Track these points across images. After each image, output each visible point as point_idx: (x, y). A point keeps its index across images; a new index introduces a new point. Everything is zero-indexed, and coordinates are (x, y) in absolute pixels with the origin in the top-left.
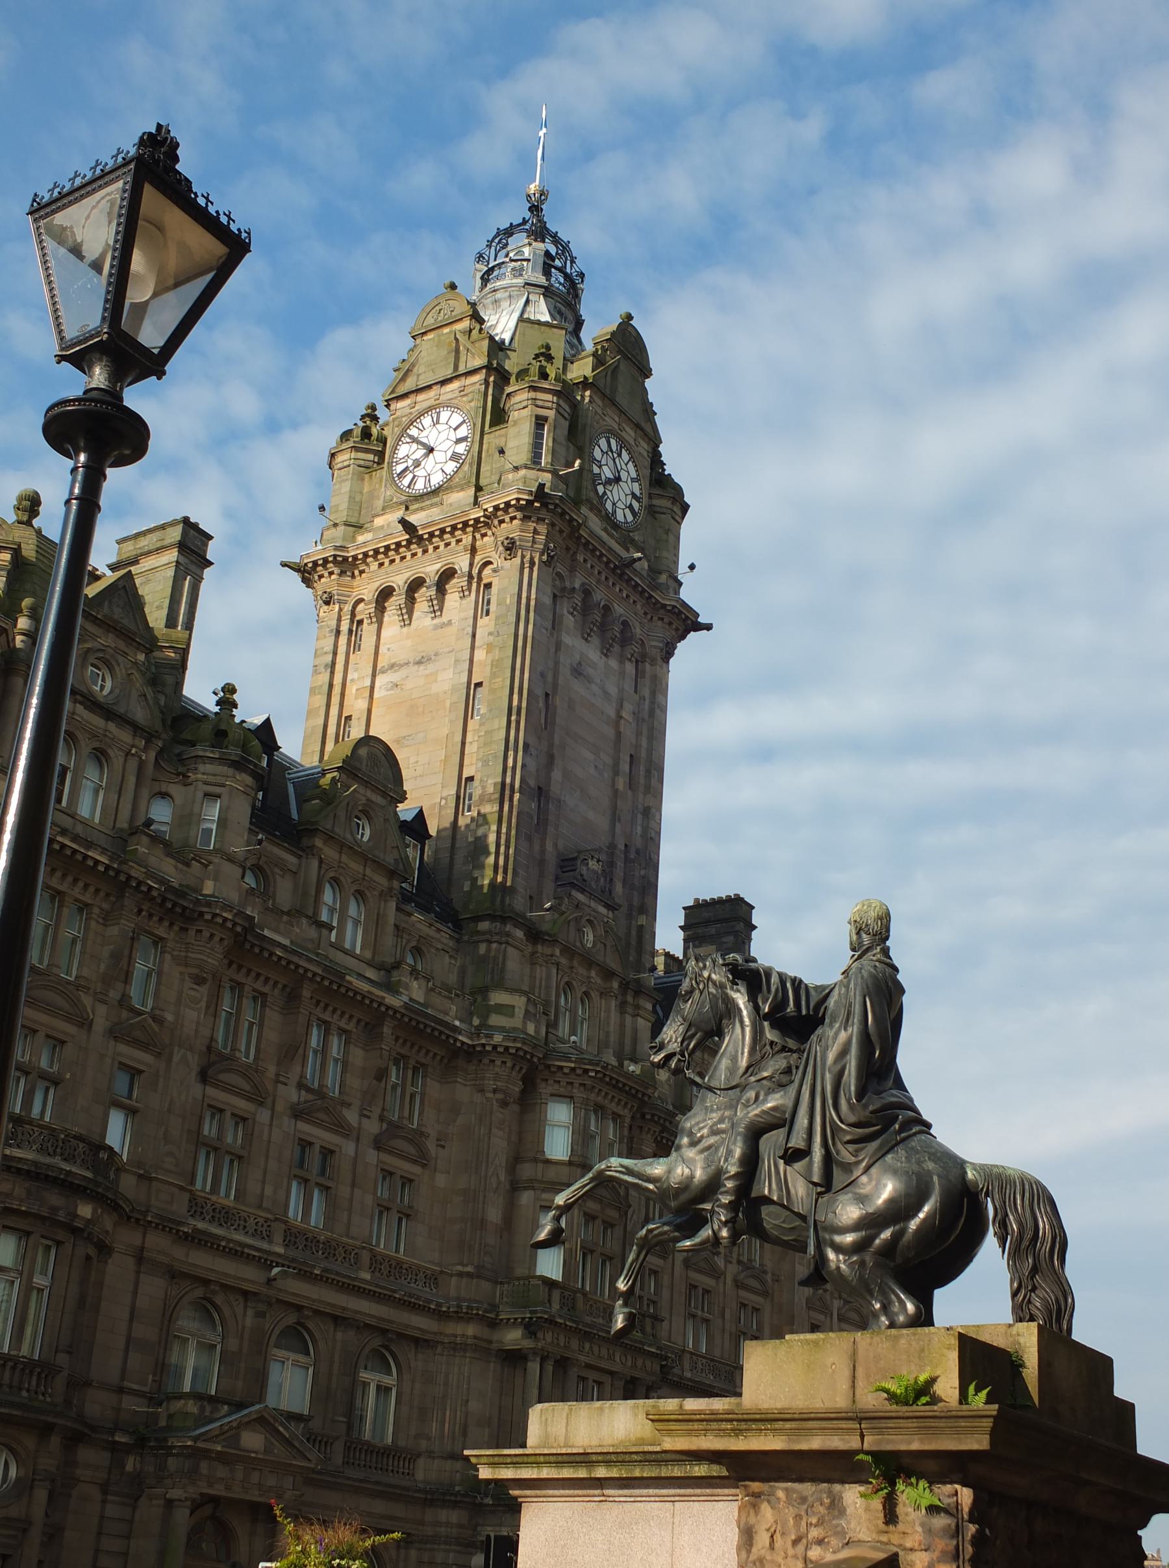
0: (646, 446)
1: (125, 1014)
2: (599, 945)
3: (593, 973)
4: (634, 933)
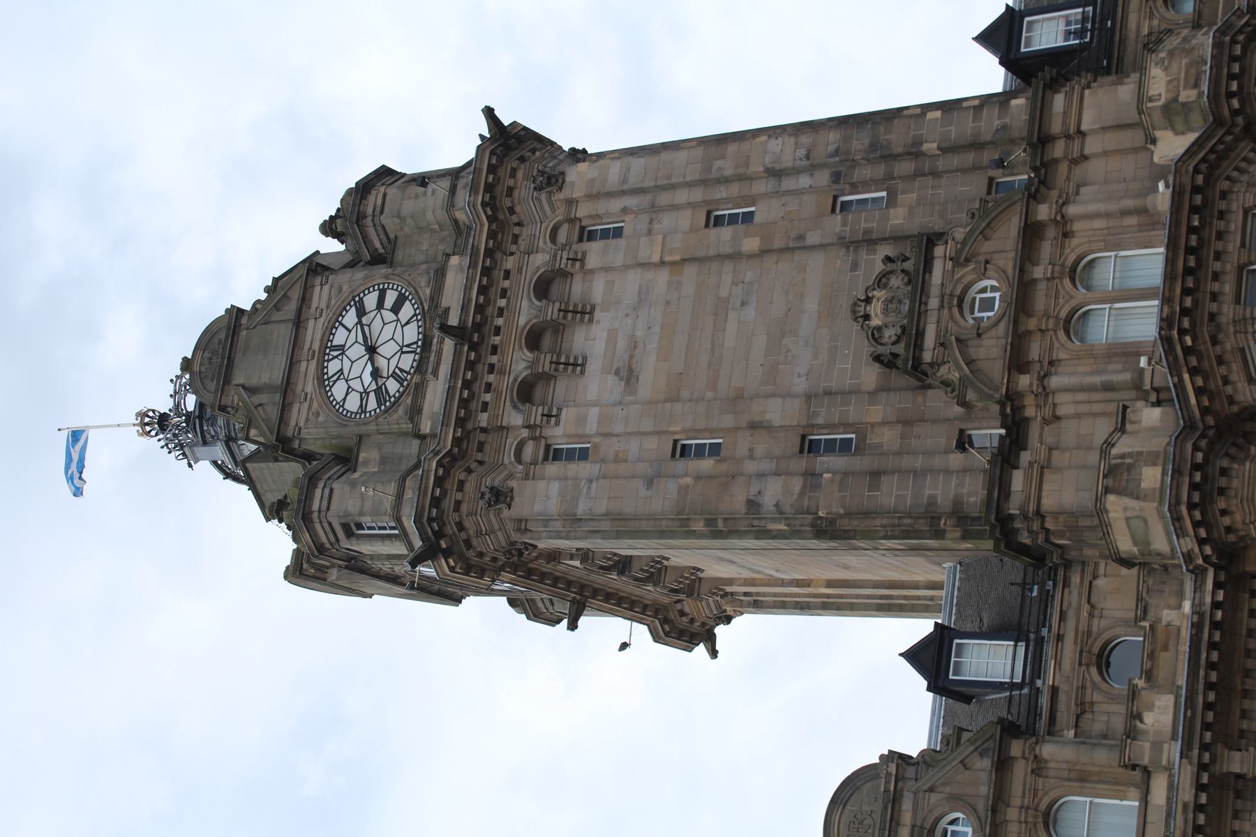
0: (317, 289)
2: (989, 273)
3: (1038, 272)
4: (956, 161)
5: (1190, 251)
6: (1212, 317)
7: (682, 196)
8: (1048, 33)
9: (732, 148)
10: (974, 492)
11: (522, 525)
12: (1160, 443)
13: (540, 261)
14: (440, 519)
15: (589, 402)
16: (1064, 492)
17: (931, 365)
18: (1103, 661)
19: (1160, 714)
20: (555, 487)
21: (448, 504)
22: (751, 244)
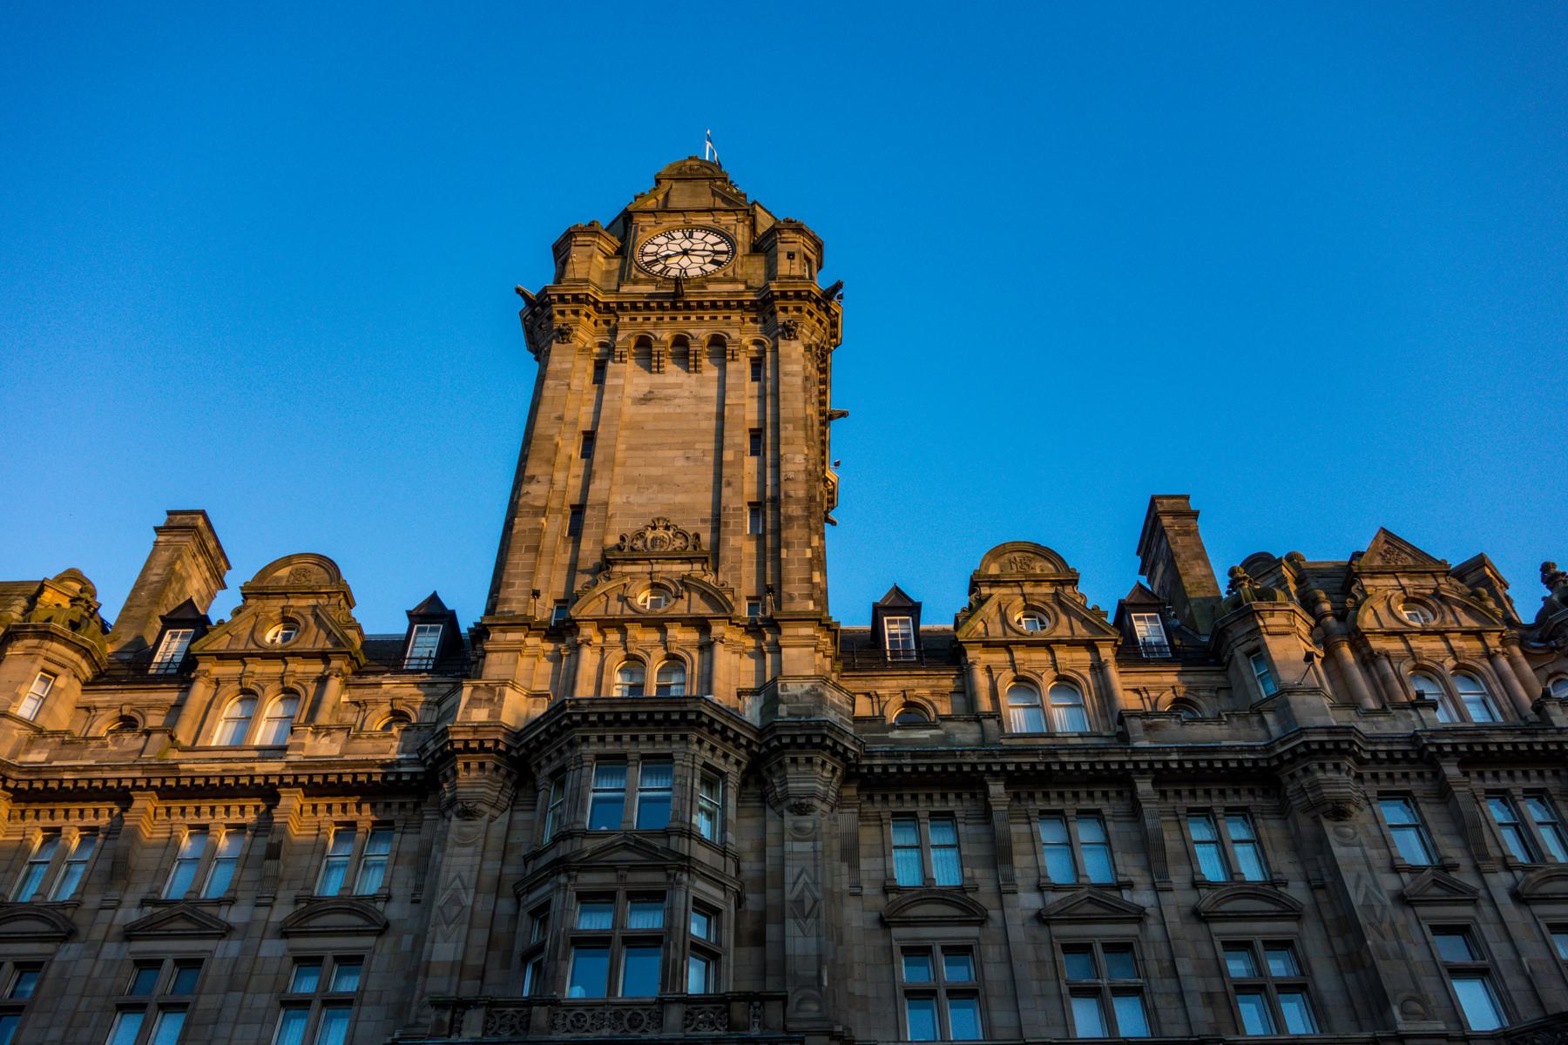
6: (585, 739)
15: (628, 377)
19: (328, 748)
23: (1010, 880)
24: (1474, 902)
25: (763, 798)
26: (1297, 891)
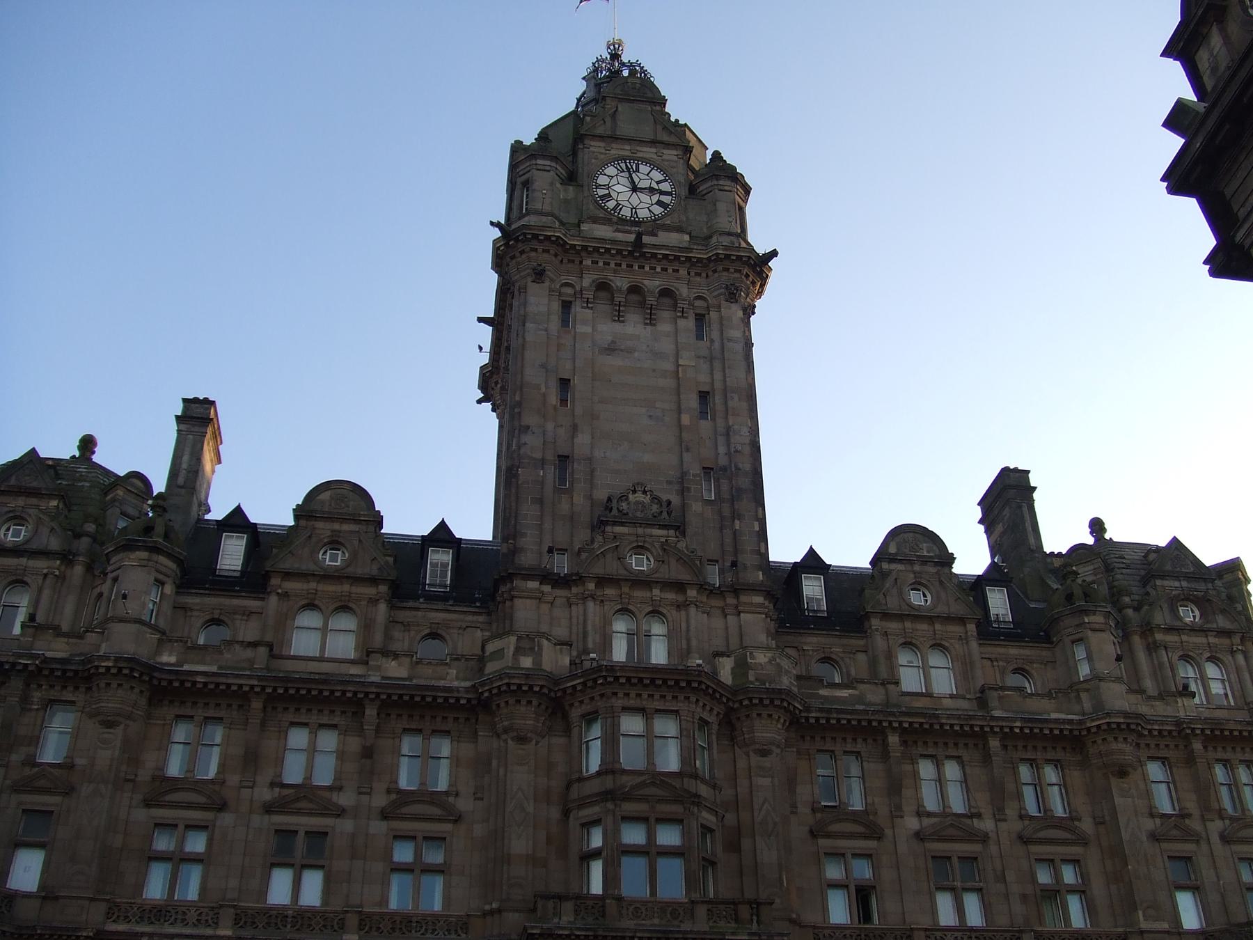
0: (675, 152)
1: (27, 771)
3: (656, 592)
4: (728, 540)
5: (653, 680)
6: (615, 694)
7: (718, 376)
8: (812, 588)
9: (745, 405)
10: (527, 559)
11: (523, 290)
12: (547, 665)
13: (684, 291)
14: (526, 240)
15: (594, 326)
16: (525, 613)
17: (604, 532)
18: (434, 635)
19: (396, 669)
20: (544, 309)
21: (535, 244)
22: (686, 419)
23: (899, 807)
24: (1198, 842)
25: (732, 739)
26: (1086, 825)
